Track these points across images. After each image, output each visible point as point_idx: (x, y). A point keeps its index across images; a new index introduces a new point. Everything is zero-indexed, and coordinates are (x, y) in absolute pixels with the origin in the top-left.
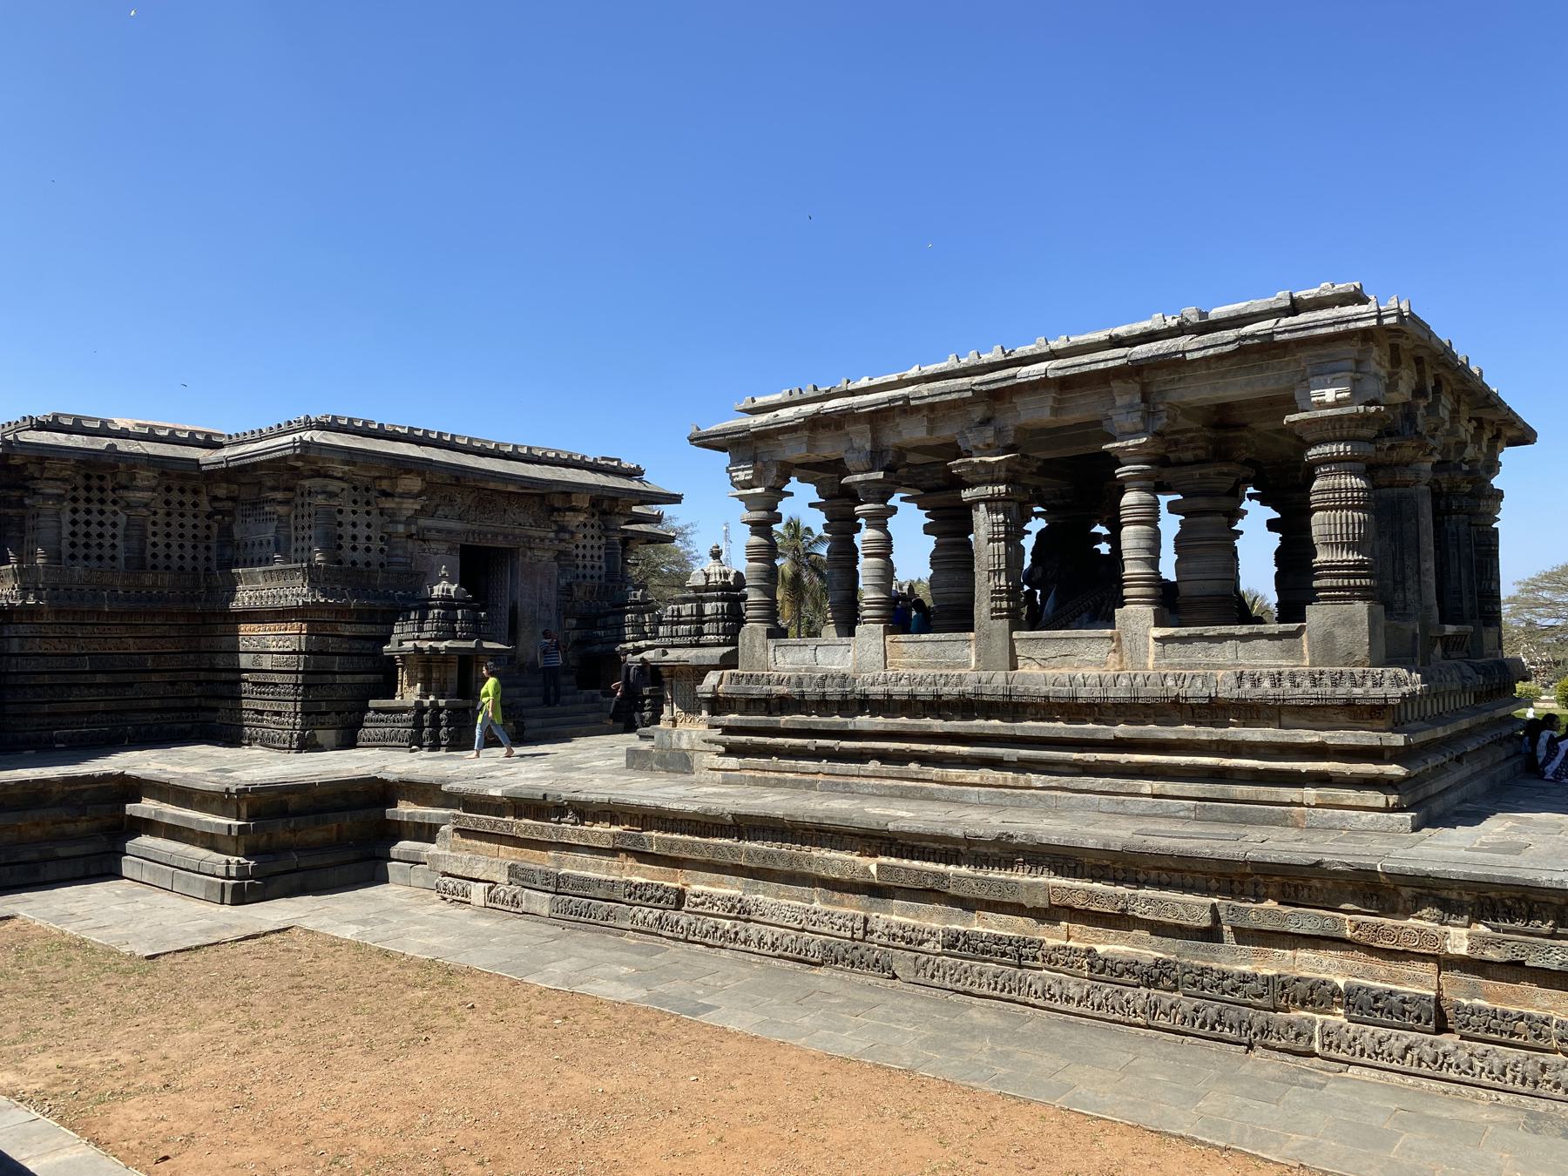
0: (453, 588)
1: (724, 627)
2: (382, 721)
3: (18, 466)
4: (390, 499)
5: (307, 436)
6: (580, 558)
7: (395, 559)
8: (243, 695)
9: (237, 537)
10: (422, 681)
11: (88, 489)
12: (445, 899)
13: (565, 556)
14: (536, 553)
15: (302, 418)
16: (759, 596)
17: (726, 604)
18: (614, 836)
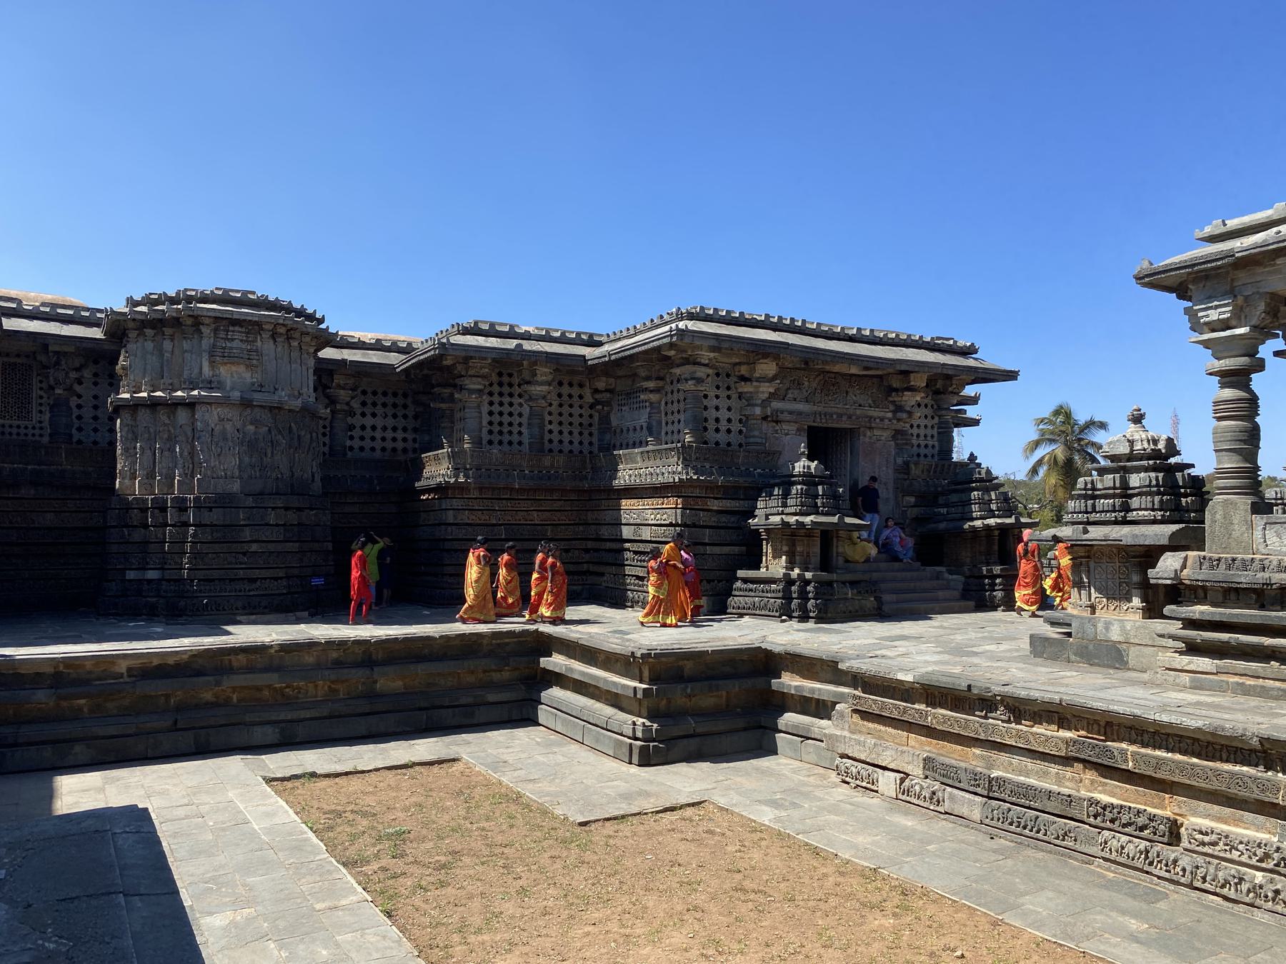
0: (814, 465)
1: (1161, 501)
2: (751, 590)
3: (448, 367)
4: (748, 383)
5: (681, 325)
6: (915, 437)
7: (752, 440)
8: (626, 563)
9: (614, 422)
10: (787, 554)
11: (501, 384)
12: (848, 783)
13: (902, 435)
14: (876, 432)
15: (674, 310)
16: (1238, 462)
17: (1161, 475)
18: (1067, 742)
